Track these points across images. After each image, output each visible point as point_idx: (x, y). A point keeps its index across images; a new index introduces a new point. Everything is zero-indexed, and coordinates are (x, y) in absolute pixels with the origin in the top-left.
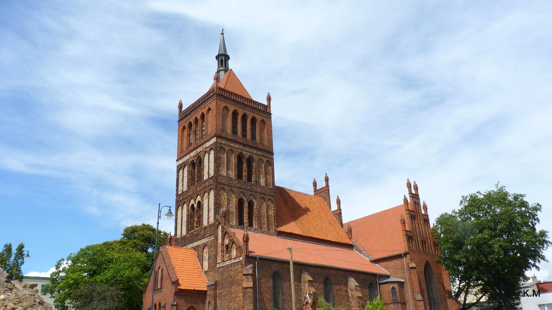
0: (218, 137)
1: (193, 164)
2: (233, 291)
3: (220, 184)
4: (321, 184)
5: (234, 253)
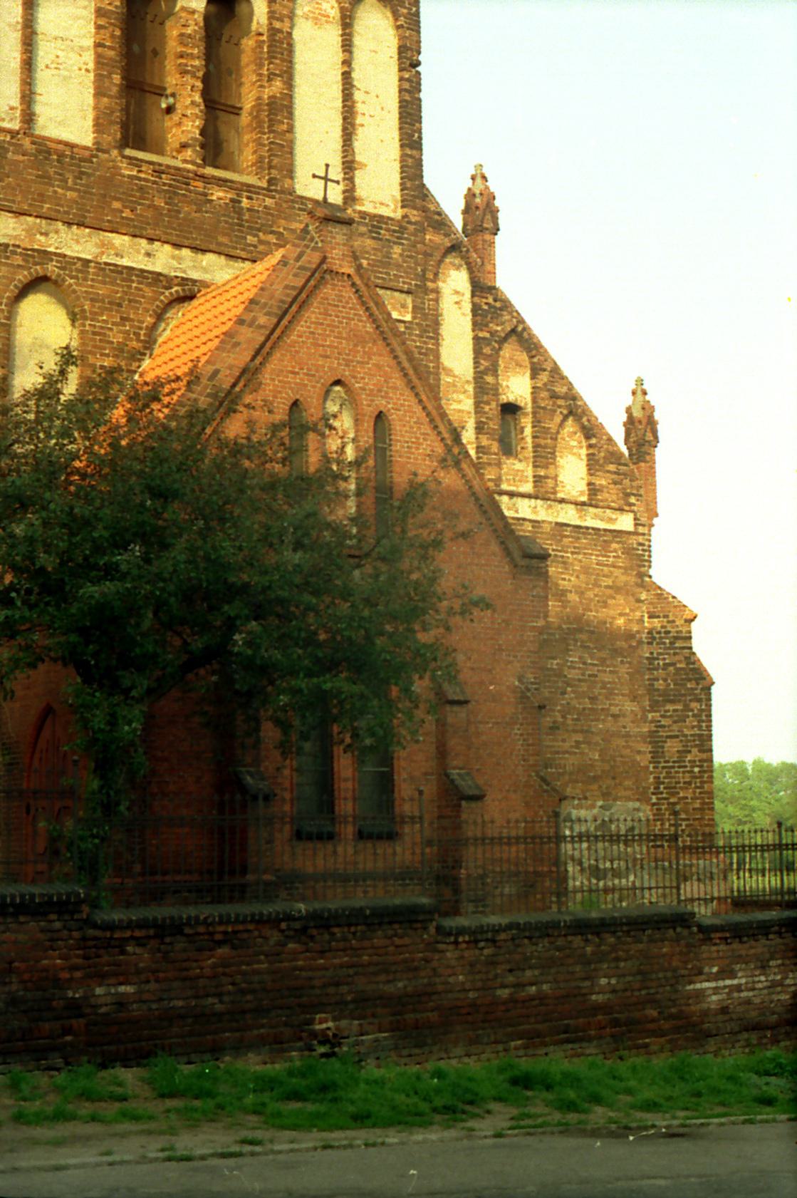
2: (572, 674)
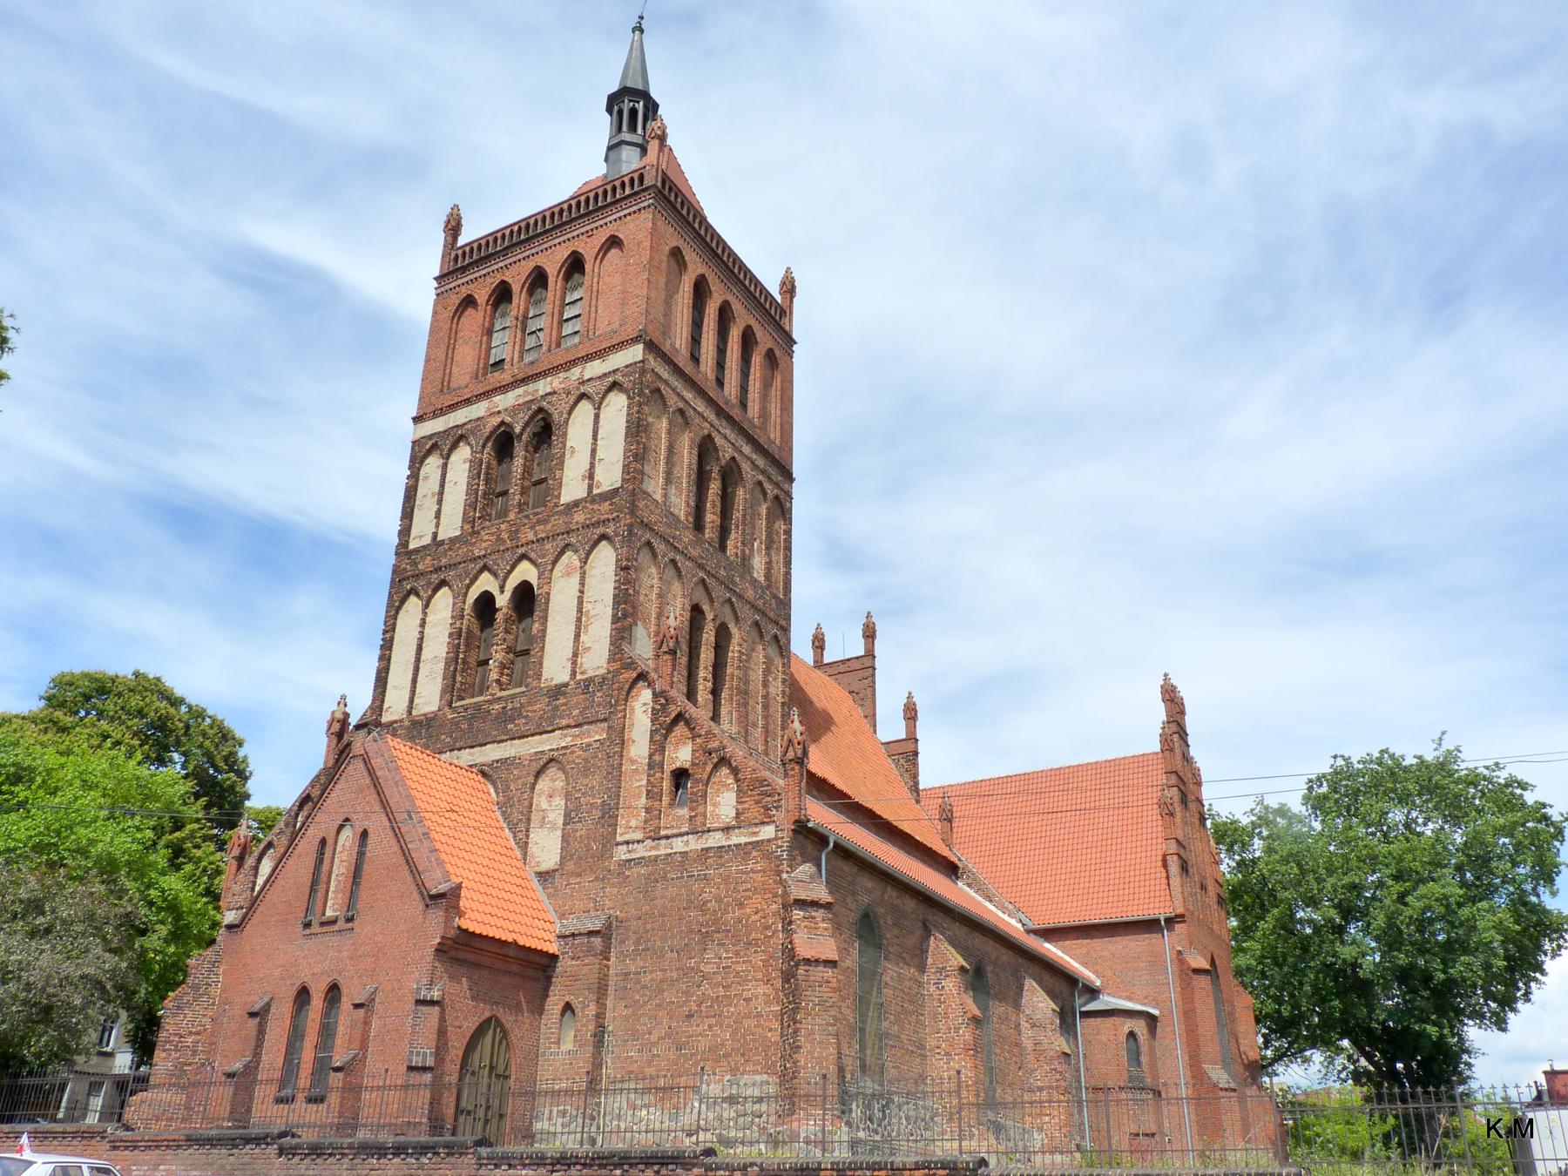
0: (652, 347)
1: (503, 442)
2: (706, 969)
3: (646, 526)
4: (844, 645)
5: (724, 803)
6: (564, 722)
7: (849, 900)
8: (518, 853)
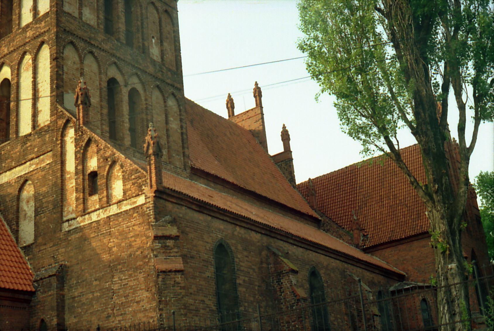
2: (116, 287)
5: (118, 188)
6: (30, 157)
7: (205, 237)
8: (13, 238)
